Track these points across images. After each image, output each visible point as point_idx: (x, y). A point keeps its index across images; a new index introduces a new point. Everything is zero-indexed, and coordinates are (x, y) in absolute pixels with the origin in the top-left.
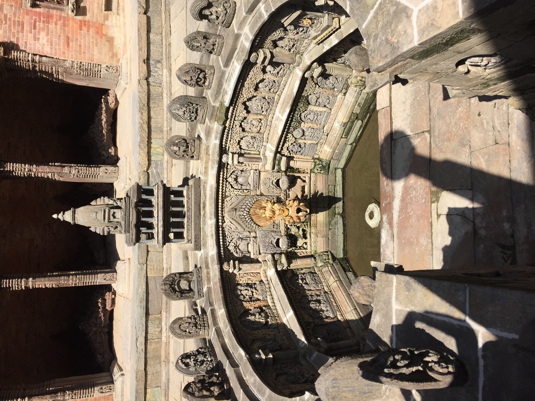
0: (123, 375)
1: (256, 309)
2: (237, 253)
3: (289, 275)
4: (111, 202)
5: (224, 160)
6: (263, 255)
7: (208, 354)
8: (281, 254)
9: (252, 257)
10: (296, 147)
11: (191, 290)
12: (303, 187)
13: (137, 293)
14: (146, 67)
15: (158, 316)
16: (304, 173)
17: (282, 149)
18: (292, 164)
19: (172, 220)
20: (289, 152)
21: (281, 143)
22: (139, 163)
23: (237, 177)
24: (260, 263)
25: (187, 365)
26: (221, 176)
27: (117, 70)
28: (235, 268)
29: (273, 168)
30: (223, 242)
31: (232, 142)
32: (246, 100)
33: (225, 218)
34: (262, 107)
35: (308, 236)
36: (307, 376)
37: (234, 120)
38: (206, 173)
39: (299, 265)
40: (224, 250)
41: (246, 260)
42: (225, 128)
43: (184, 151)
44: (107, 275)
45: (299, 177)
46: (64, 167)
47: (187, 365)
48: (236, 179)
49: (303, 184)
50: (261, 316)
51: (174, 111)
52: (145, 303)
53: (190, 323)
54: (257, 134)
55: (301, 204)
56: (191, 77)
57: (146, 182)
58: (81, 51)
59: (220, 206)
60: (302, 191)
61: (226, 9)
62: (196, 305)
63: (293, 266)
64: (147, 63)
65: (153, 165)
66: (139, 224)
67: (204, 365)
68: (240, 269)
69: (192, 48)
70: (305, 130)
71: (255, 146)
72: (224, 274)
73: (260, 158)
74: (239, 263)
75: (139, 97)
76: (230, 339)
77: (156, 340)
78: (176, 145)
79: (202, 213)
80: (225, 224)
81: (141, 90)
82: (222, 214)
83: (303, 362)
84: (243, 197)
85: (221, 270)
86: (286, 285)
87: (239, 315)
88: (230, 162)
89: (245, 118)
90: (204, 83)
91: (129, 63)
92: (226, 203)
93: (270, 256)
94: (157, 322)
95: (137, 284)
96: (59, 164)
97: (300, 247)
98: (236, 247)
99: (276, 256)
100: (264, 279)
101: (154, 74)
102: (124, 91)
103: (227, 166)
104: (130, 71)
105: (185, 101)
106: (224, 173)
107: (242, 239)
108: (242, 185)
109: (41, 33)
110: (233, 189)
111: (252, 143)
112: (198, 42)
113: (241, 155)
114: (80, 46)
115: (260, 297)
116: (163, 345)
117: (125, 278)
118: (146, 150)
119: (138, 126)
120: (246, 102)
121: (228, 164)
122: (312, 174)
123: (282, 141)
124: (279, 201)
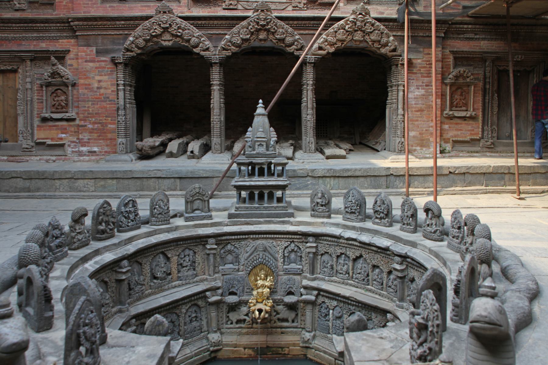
0: (132, 160)
2: (225, 253)
4: (272, 143)
5: (311, 239)
6: (222, 278)
10: (325, 311)
11: (193, 211)
13: (199, 170)
15: (178, 188)
17: (323, 296)
19: (256, 192)
20: (321, 304)
21: (327, 295)
25: (126, 205)
26: (295, 237)
27: (401, 151)
30: (235, 239)
31: (327, 246)
33: (256, 241)
43: (318, 203)
45: (297, 315)
46: (312, 109)
47: (126, 205)
52: (191, 176)
54: (335, 271)
57: (299, 175)
70: (342, 319)
71: (326, 270)
72: (205, 240)
77: (157, 187)
78: (323, 196)
79: (261, 220)
80: (251, 241)
82: (260, 238)
87: (166, 252)
88: (308, 245)
92: (271, 241)
93: (219, 284)
94: (173, 187)
95: (208, 169)
96: (315, 106)
109: (423, 90)
111: (326, 266)
117: (215, 160)
121: (307, 243)
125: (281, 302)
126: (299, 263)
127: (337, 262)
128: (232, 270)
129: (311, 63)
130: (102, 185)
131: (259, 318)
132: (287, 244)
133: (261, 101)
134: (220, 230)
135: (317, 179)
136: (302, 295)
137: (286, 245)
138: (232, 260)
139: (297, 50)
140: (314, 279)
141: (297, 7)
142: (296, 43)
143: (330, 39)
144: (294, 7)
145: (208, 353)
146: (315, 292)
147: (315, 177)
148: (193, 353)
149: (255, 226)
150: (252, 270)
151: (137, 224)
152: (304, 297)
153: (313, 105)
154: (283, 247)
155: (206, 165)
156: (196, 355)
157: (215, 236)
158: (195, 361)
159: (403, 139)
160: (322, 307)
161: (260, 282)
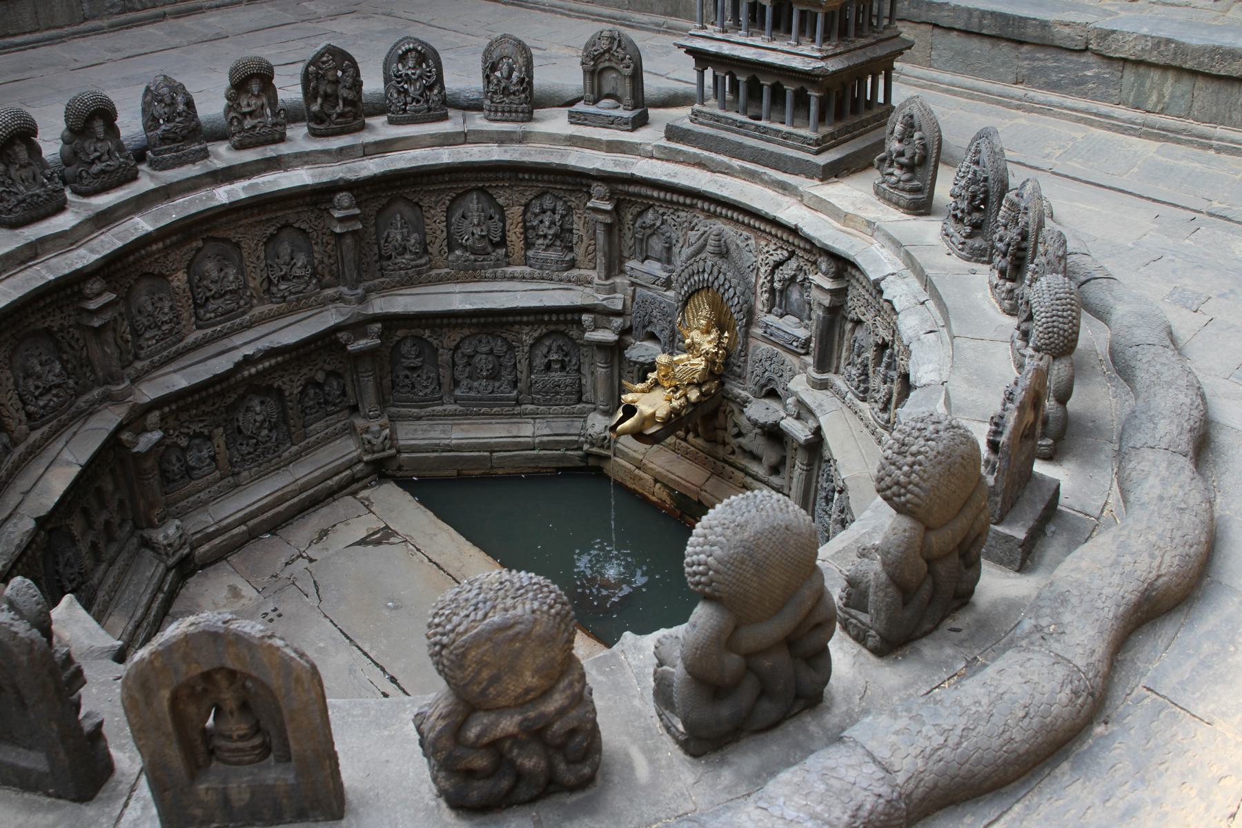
9: (630, 264)
22: (1114, 32)
30: (665, 201)
33: (712, 221)
36: (283, 287)
65: (1106, 72)
72: (584, 181)
74: (606, 225)
76: (415, 158)
79: (736, 163)
80: (702, 217)
83: (330, 292)
86: (539, 317)
92: (745, 233)
99: (617, 322)
110: (772, 263)
132: (781, 255)
134: (625, 165)
135: (1117, 65)
137: (776, 258)
145: (580, 453)
147: (1111, 58)
148: (537, 440)
149: (718, 177)
151: (429, 109)
156: (544, 446)
157: (609, 179)
158: (539, 457)
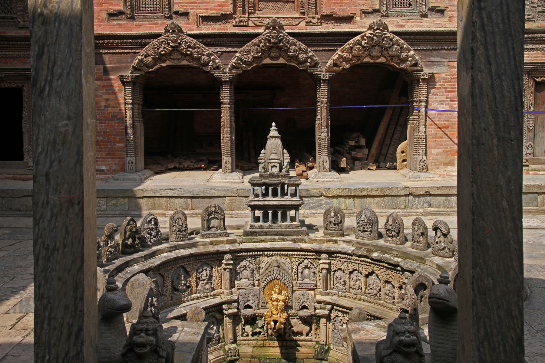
1: (189, 282)
2: (240, 268)
3: (218, 315)
5: (323, 256)
6: (238, 292)
7: (156, 239)
8: (238, 308)
9: (236, 282)
11: (209, 228)
12: (301, 334)
13: (211, 189)
14: (422, 193)
15: (190, 207)
16: (316, 334)
17: (336, 310)
18: (323, 320)
19: (270, 212)
21: (341, 309)
23: (309, 268)
24: (230, 289)
26: (309, 253)
27: (422, 169)
28: (226, 265)
29: (318, 302)
30: (250, 256)
31: (339, 262)
32: (376, 273)
34: (372, 289)
35: (255, 337)
37: (359, 264)
38: (312, 241)
39: (227, 326)
40: (242, 256)
41: (234, 276)
42: (352, 256)
43: (331, 222)
44: (230, 165)
48: (306, 267)
49: (304, 333)
50: (183, 286)
51: (364, 212)
52: (203, 195)
53: (182, 226)
54: (348, 286)
55: (282, 326)
56: (391, 225)
58: (436, 138)
59: (282, 253)
60: (297, 332)
61: (443, 249)
62: (196, 234)
63: (227, 320)
64: (427, 195)
65: (329, 200)
66: (267, 186)
67: (148, 236)
68: (225, 269)
69: (414, 224)
71: (338, 285)
72: (221, 255)
73: (327, 289)
74: (230, 269)
75: (392, 188)
76: (165, 257)
77: (169, 206)
78: (336, 215)
79: (276, 237)
81: (399, 189)
82: (275, 255)
84: (290, 274)
85: (225, 253)
88: (321, 261)
89: (361, 274)
90: (389, 236)
91: (430, 179)
92: (285, 258)
93: (236, 298)
94: (184, 206)
97: (244, 329)
98: (245, 267)
99: (235, 304)
100: (215, 292)
101: (416, 201)
102: (404, 176)
103: (318, 259)
104: (422, 181)
105: (373, 222)
106: (312, 256)
107: (252, 273)
108: (302, 273)
112: (419, 229)
113: (329, 270)
114: (441, 138)
115: (199, 287)
116: (164, 212)
117: (226, 179)
118: (342, 195)
119: (365, 187)
120: (375, 273)
121: (320, 259)
122: (314, 343)
123: (343, 310)
124: (287, 307)
125: (295, 316)
126: (312, 279)
127: (350, 278)
128: (247, 285)
129: (326, 80)
130: (113, 204)
131: (274, 328)
132: (301, 260)
133: (274, 124)
136: (315, 309)
138: (247, 275)
139: (310, 67)
140: (328, 294)
141: (311, 22)
142: (309, 60)
143: (345, 55)
144: (307, 22)
146: (329, 307)
150: (267, 284)
152: (317, 311)
153: (327, 123)
154: (297, 264)
155: (218, 185)
157: (231, 252)
159: (424, 157)
160: (335, 321)
161: (275, 296)
